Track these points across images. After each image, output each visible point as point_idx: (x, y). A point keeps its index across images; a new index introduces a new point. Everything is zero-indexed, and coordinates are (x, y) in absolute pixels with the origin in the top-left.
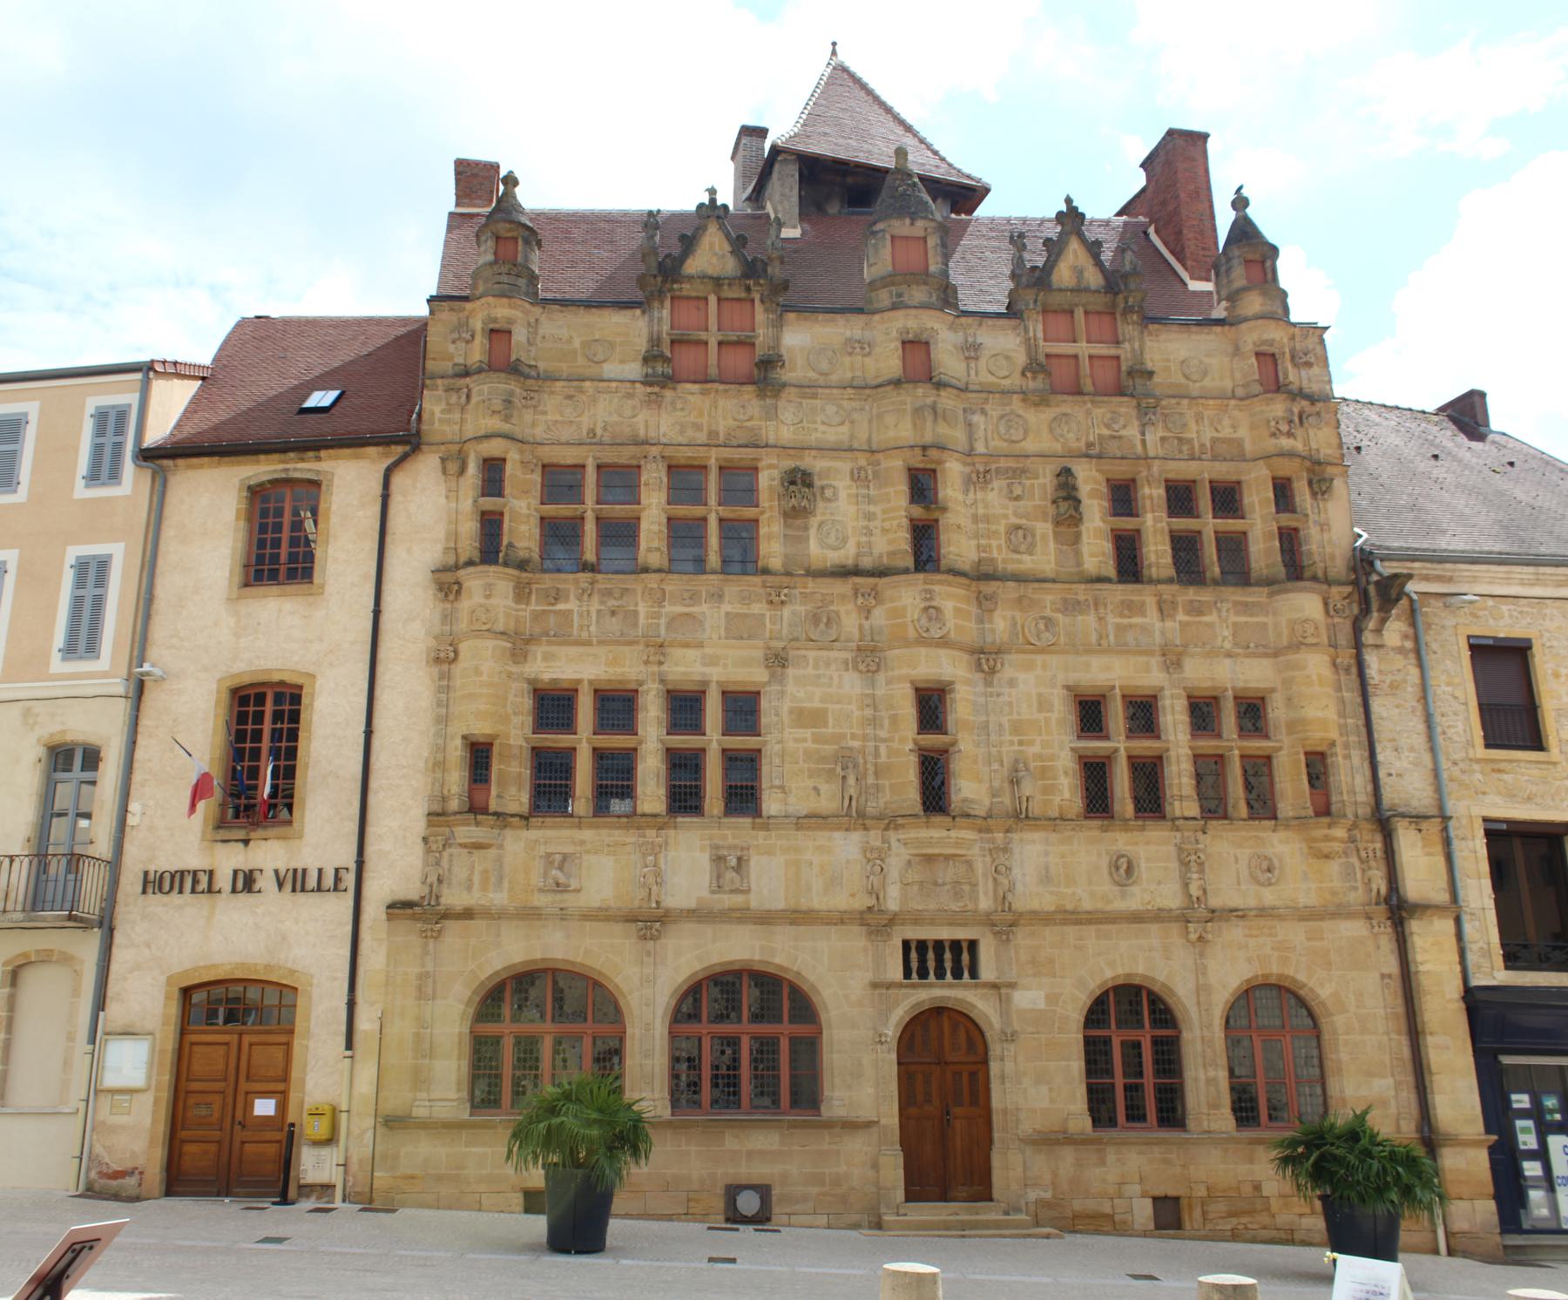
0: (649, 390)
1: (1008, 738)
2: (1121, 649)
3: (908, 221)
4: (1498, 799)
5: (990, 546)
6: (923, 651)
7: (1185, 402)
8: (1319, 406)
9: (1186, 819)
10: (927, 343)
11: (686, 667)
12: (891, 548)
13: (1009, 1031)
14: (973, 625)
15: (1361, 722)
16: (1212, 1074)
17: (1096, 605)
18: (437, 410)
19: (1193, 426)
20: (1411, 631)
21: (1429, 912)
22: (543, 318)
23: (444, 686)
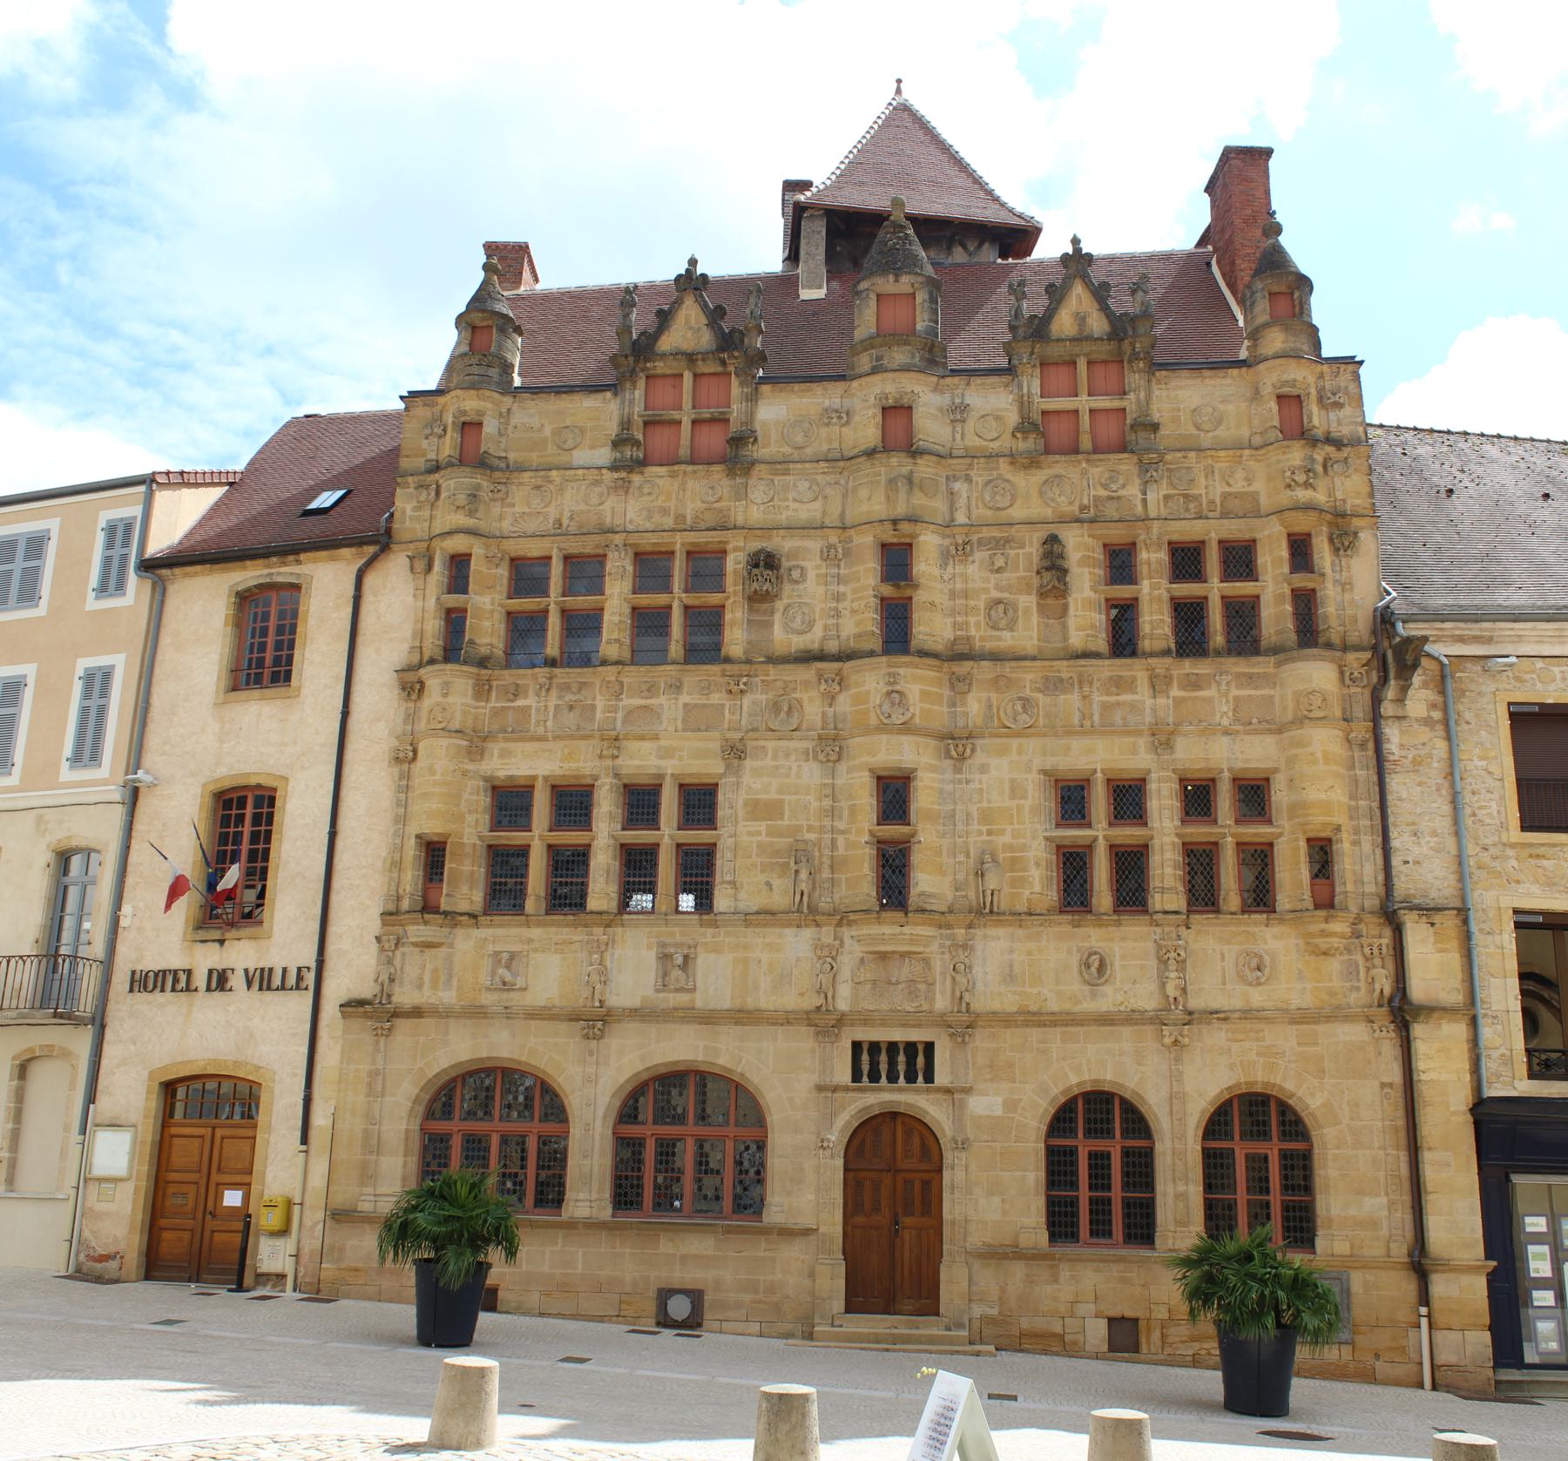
0: (616, 475)
1: (976, 827)
2: (1107, 729)
3: (891, 278)
4: (1535, 889)
5: (967, 623)
6: (884, 737)
7: (1192, 455)
8: (1346, 451)
9: (1166, 912)
10: (910, 408)
11: (641, 760)
12: (857, 630)
14: (945, 709)
15: (1376, 805)
16: (1181, 1188)
17: (1080, 683)
18: (408, 507)
19: (1203, 482)
20: (1440, 699)
21: (1436, 1015)
22: (515, 407)
23: (404, 787)
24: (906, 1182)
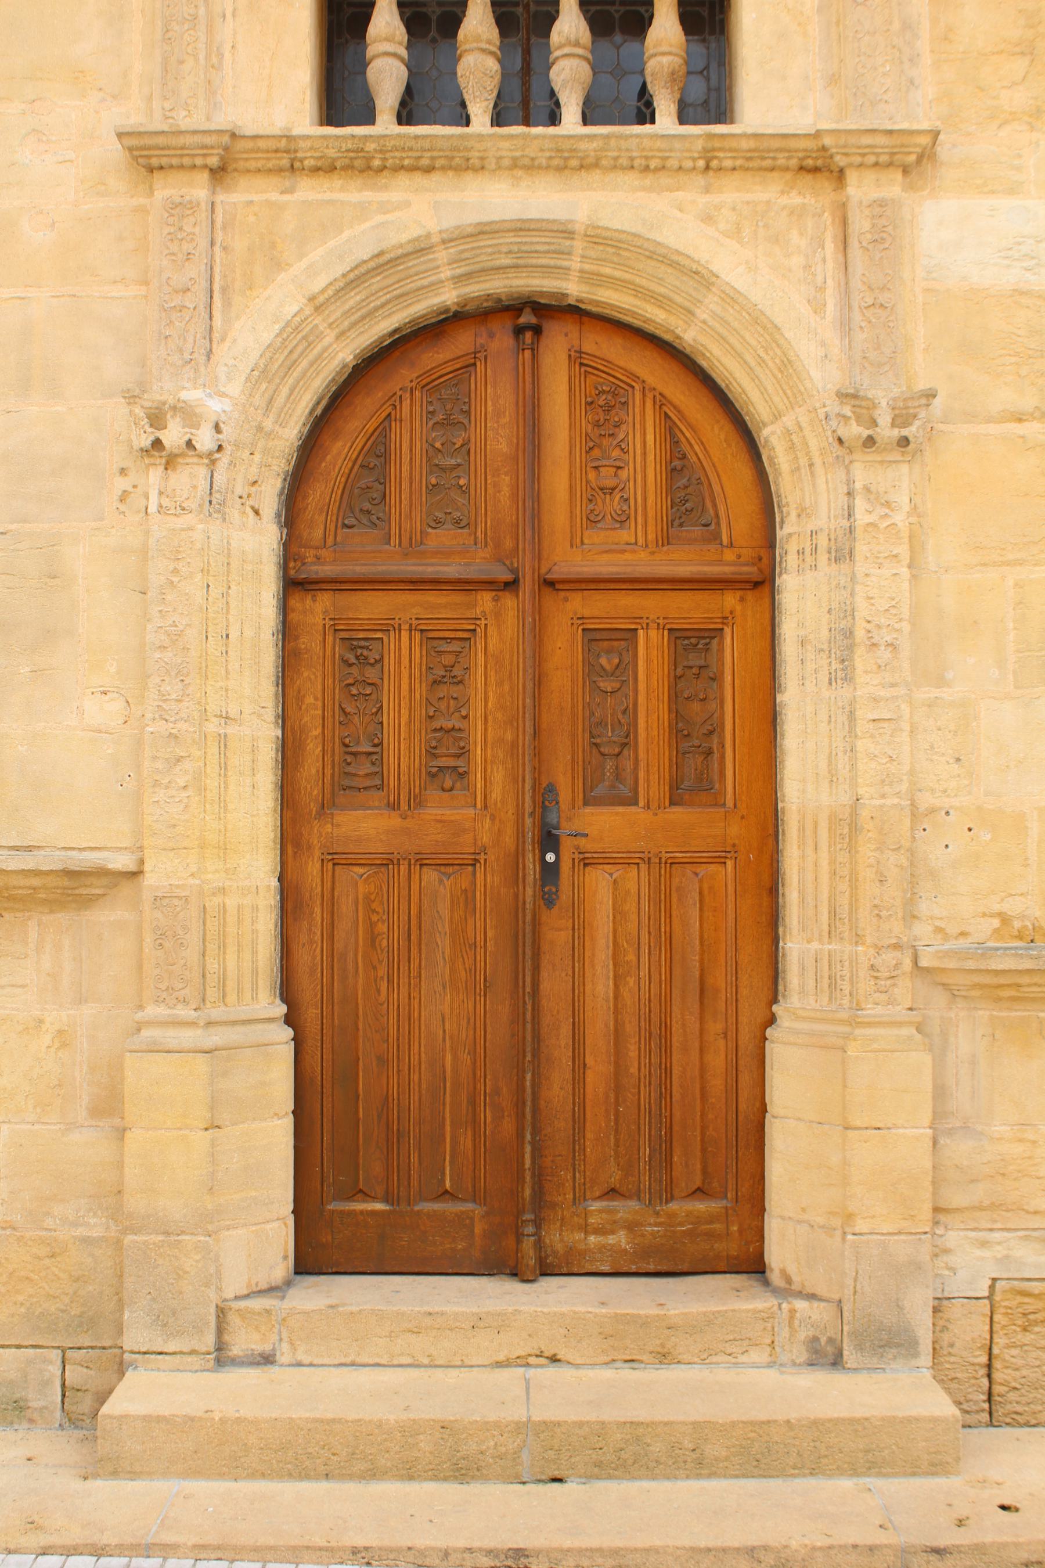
13: (883, 395)
24: (595, 637)
